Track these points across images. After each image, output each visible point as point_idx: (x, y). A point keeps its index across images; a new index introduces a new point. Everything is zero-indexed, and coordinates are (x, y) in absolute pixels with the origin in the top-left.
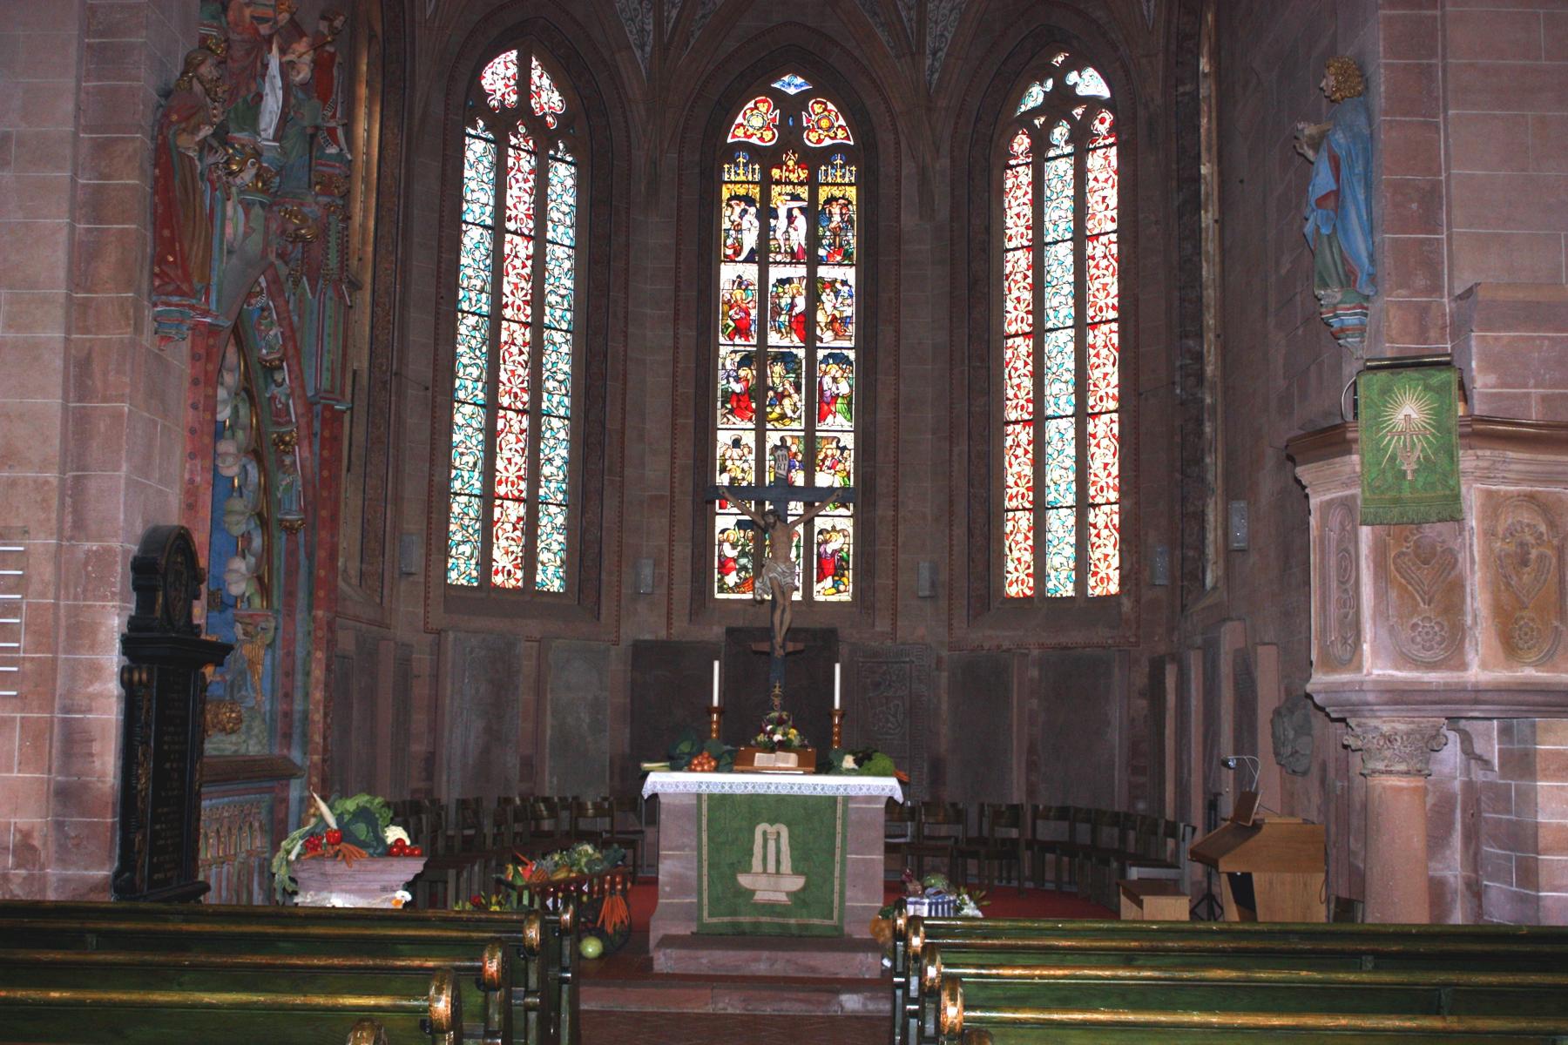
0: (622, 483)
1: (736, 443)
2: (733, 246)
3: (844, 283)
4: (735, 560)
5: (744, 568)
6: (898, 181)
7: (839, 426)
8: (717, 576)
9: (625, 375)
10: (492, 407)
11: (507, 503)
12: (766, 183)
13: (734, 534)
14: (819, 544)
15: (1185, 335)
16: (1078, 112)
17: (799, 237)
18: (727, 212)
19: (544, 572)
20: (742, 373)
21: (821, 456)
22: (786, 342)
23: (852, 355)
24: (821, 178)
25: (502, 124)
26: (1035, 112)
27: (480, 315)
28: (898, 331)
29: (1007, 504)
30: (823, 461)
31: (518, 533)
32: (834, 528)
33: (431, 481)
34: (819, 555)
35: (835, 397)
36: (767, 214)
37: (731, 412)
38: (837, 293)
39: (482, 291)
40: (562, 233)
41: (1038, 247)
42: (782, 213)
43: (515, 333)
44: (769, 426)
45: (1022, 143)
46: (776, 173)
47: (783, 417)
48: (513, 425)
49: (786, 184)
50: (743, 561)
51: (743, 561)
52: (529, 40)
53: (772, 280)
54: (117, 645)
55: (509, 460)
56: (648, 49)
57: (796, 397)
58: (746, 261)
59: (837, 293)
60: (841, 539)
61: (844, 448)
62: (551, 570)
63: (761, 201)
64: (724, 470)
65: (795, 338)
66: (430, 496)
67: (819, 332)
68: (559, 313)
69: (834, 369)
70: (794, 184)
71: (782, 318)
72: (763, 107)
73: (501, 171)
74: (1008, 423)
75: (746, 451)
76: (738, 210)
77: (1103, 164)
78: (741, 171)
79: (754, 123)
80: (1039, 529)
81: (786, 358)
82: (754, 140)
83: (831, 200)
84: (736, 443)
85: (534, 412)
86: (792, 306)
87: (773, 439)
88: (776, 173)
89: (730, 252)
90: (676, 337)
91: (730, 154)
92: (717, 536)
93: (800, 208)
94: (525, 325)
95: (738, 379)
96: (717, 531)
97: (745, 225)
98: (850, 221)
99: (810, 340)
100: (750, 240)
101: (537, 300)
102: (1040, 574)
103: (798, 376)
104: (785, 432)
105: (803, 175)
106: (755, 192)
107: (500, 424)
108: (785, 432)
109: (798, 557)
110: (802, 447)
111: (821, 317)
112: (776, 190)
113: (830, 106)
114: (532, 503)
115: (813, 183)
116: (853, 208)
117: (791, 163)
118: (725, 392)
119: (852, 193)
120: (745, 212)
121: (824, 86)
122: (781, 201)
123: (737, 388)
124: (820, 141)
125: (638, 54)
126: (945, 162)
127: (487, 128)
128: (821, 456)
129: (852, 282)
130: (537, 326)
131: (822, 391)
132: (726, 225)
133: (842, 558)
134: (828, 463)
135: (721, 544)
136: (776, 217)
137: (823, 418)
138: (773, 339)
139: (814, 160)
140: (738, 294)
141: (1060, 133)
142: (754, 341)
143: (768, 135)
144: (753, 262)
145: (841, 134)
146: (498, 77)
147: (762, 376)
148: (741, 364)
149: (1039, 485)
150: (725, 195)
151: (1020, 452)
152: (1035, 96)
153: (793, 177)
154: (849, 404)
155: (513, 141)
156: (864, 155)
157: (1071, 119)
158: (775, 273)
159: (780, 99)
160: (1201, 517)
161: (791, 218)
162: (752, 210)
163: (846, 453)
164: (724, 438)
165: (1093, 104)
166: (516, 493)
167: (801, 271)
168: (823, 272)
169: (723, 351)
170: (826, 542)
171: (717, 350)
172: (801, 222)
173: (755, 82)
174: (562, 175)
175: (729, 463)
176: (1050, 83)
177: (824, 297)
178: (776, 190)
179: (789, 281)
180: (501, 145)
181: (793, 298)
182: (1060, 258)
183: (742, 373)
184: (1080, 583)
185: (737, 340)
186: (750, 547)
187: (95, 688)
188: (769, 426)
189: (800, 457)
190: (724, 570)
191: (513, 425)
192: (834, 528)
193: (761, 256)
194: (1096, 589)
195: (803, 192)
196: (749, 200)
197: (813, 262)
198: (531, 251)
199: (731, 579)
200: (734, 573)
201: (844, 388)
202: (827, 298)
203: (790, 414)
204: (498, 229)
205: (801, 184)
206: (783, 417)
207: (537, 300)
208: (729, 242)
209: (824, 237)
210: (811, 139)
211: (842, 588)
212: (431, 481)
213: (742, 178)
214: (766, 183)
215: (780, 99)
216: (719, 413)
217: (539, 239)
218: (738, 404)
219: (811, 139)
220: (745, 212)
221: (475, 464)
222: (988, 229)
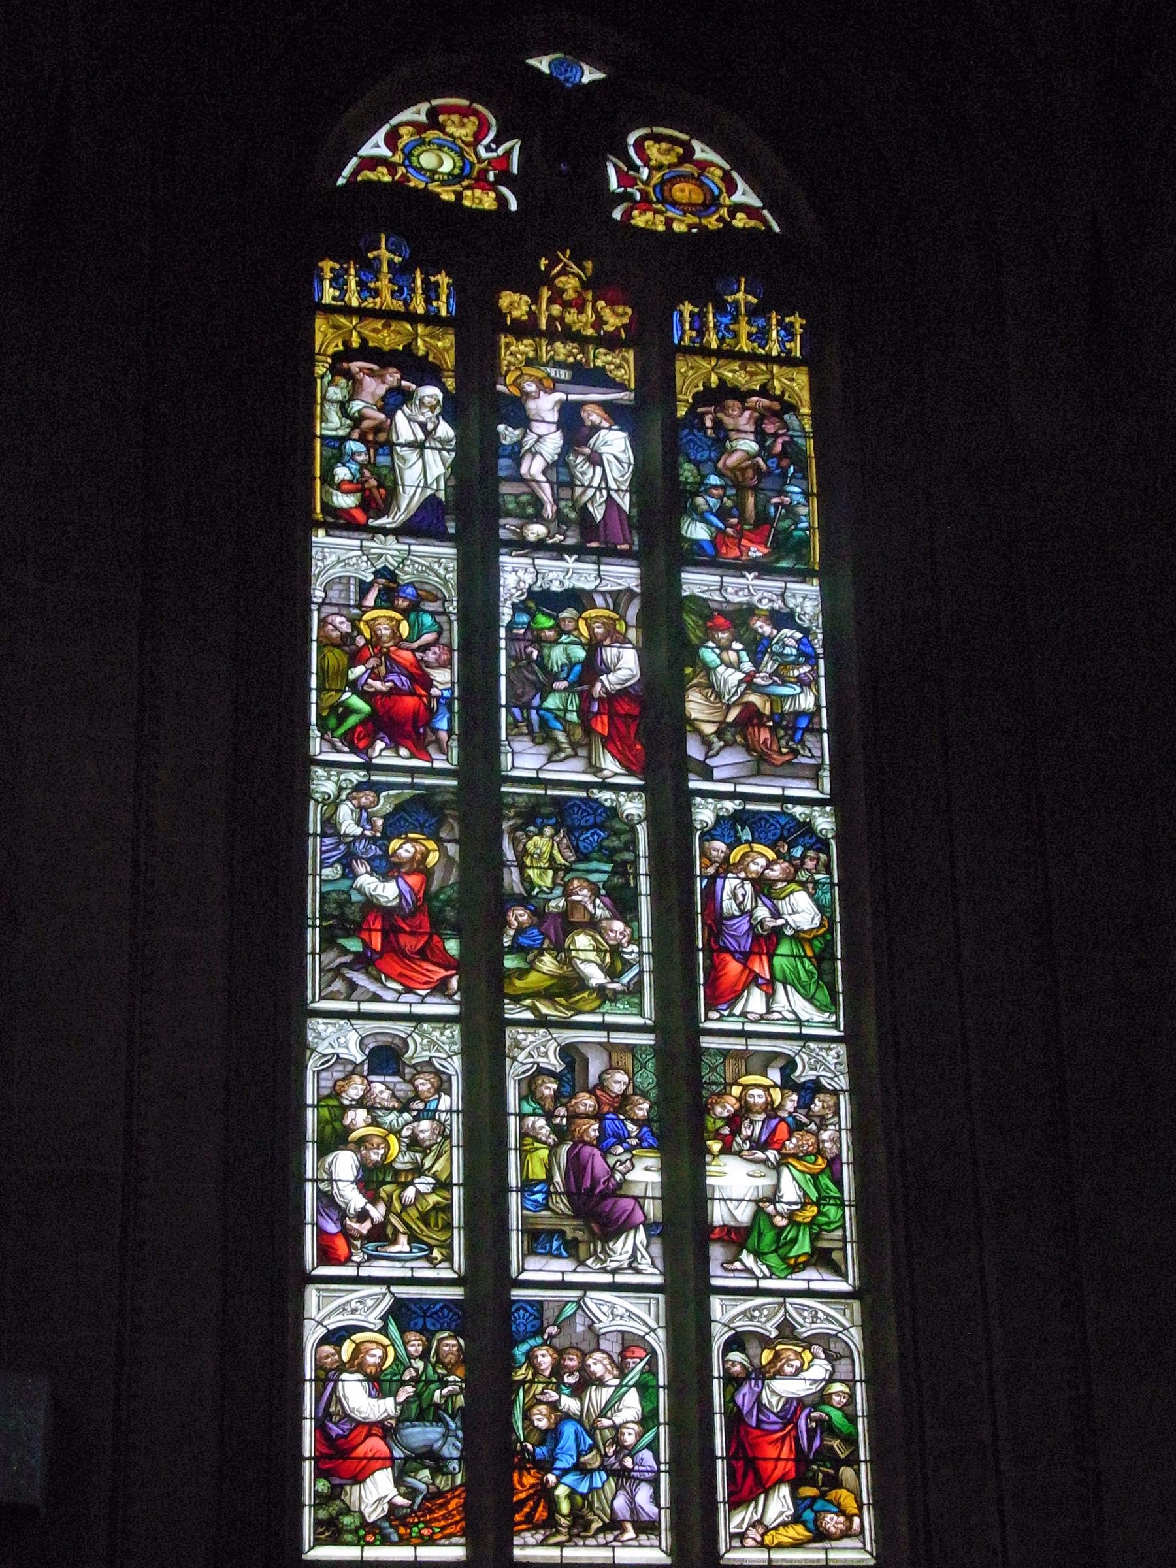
2: (356, 485)
4: (385, 1430)
5: (431, 1458)
7: (786, 1020)
8: (310, 1484)
14: (732, 1381)
20: (404, 850)
21: (726, 1108)
22: (571, 771)
23: (824, 823)
30: (735, 1121)
32: (787, 1331)
34: (735, 1418)
37: (363, 961)
38: (758, 648)
44: (513, 1012)
49: (552, 335)
50: (423, 1435)
51: (423, 1435)
60: (820, 1370)
61: (815, 1088)
63: (461, 371)
64: (335, 1138)
65: (610, 764)
67: (694, 749)
71: (552, 702)
72: (463, 131)
75: (424, 1085)
76: (374, 388)
78: (384, 284)
86: (593, 668)
87: (532, 1050)
93: (605, 406)
96: (312, 1334)
97: (404, 428)
98: (792, 452)
100: (423, 474)
103: (624, 870)
104: (593, 1011)
109: (647, 1420)
110: (647, 1079)
116: (803, 421)
117: (570, 284)
123: (387, 892)
128: (726, 1108)
131: (716, 921)
133: (827, 1427)
134: (754, 1128)
135: (327, 1377)
136: (523, 421)
137: (723, 996)
138: (523, 759)
144: (440, 536)
150: (325, 336)
154: (823, 958)
161: (572, 423)
167: (624, 575)
169: (324, 784)
170: (761, 1374)
171: (307, 777)
178: (514, 351)
179: (578, 599)
181: (594, 646)
183: (404, 850)
186: (451, 1389)
190: (342, 1458)
192: (787, 1331)
195: (622, 365)
199: (377, 1492)
201: (801, 911)
203: (596, 976)
205: (611, 342)
206: (569, 985)
209: (701, 488)
211: (833, 1522)
213: (387, 301)
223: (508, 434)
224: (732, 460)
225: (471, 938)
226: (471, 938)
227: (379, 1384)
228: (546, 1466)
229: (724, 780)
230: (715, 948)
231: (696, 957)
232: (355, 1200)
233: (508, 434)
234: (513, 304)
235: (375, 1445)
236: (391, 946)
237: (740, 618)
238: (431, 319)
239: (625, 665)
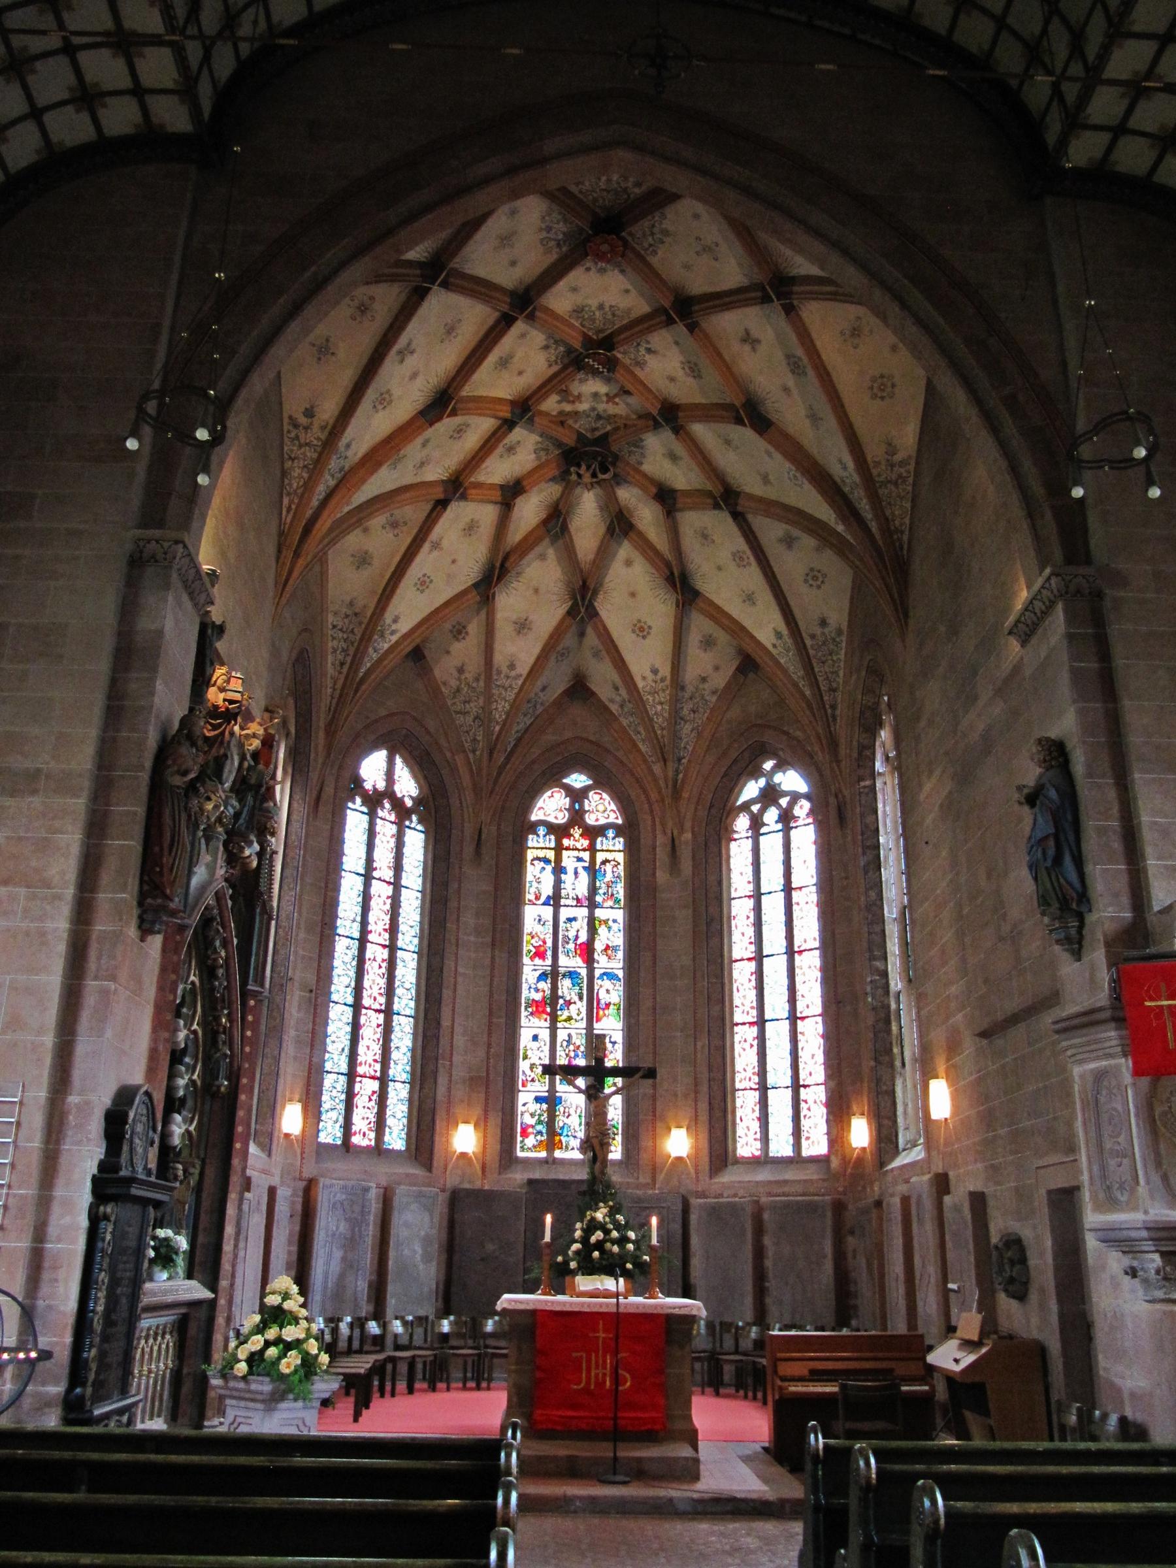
0: (451, 1065)
1: (535, 1038)
3: (615, 921)
5: (540, 1133)
6: (654, 848)
8: (519, 1139)
9: (455, 985)
10: (357, 1006)
11: (364, 1080)
12: (559, 849)
13: (534, 1107)
15: (872, 958)
16: (784, 802)
17: (582, 889)
18: (529, 868)
19: (391, 1133)
23: (620, 974)
24: (598, 847)
25: (373, 801)
26: (752, 801)
27: (352, 938)
28: (654, 956)
29: (738, 1085)
31: (373, 1103)
33: (311, 1061)
35: (608, 1005)
36: (559, 870)
37: (532, 1014)
38: (609, 928)
39: (354, 921)
40: (413, 877)
41: (757, 896)
42: (570, 871)
43: (376, 953)
45: (742, 823)
46: (566, 842)
47: (569, 1019)
48: (372, 1022)
50: (539, 1127)
51: (539, 1127)
52: (396, 744)
53: (562, 918)
54: (88, 1184)
55: (368, 1047)
56: (478, 753)
57: (579, 1003)
58: (544, 904)
59: (609, 928)
62: (395, 1135)
64: (525, 1057)
66: (310, 1073)
67: (596, 956)
68: (409, 938)
69: (607, 984)
70: (577, 849)
73: (372, 834)
74: (737, 1024)
77: (805, 837)
78: (541, 840)
79: (551, 806)
80: (764, 1103)
81: (572, 975)
82: (551, 819)
83: (604, 862)
84: (535, 1038)
85: (388, 1012)
86: (577, 937)
87: (562, 1035)
88: (566, 842)
89: (532, 897)
90: (493, 958)
91: (533, 828)
92: (520, 1109)
94: (384, 946)
95: (537, 990)
96: (520, 1102)
99: (589, 960)
100: (547, 890)
101: (393, 929)
102: (765, 1139)
105: (586, 843)
106: (551, 855)
107: (363, 1020)
108: (573, 1030)
110: (584, 1041)
111: (599, 946)
112: (565, 853)
113: (605, 796)
114: (384, 1080)
115: (592, 849)
116: (621, 867)
117: (577, 836)
118: (528, 999)
119: (620, 857)
120: (544, 868)
121: (602, 781)
122: (568, 860)
123: (538, 997)
124: (597, 820)
125: (471, 756)
126: (688, 836)
127: (363, 804)
129: (620, 919)
130: (392, 948)
131: (598, 1001)
132: (529, 877)
138: (563, 961)
139: (593, 833)
140: (538, 929)
141: (771, 816)
142: (549, 961)
143: (560, 815)
145: (613, 816)
146: (373, 768)
147: (554, 988)
148: (539, 979)
149: (762, 1072)
150: (530, 854)
151: (747, 1046)
152: (751, 790)
153: (579, 846)
154: (618, 1009)
155: (380, 813)
156: (628, 830)
157: (779, 806)
158: (564, 913)
159: (569, 791)
160: (893, 1093)
161: (576, 873)
162: (549, 868)
163: (616, 1046)
164: (525, 1036)
165: (795, 797)
166: (373, 1073)
168: (599, 913)
172: (584, 877)
173: (552, 777)
174: (415, 841)
175: (529, 1053)
176: (762, 782)
177: (600, 931)
178: (565, 853)
179: (575, 919)
180: (372, 815)
182: (773, 907)
184: (797, 1145)
185: (537, 961)
186: (545, 1117)
187: (67, 1220)
188: (559, 1025)
189: (582, 1049)
190: (525, 1134)
191: (372, 1022)
193: (555, 900)
194: (808, 1150)
195: (586, 855)
196: (546, 861)
197: (592, 905)
198: (390, 893)
199: (530, 1141)
200: (532, 1137)
202: (602, 930)
203: (575, 1016)
204: (368, 876)
205: (584, 850)
207: (393, 929)
208: (533, 890)
209: (600, 888)
210: (590, 820)
212: (311, 1061)
214: (559, 849)
215: (569, 791)
216: (524, 1013)
217: (397, 885)
218: (537, 1008)
219: (590, 820)
220: (544, 868)
221: (343, 1050)
222: (720, 883)
223: (563, 876)
224: (606, 880)
225: (550, 1007)
226: (550, 1007)
227: (532, 1115)
228: (560, 1135)
229: (602, 963)
230: (598, 1008)
231: (594, 1010)
232: (528, 1072)
233: (563, 876)
235: (530, 1130)
236: (537, 1011)
237: (606, 922)
239: (583, 938)
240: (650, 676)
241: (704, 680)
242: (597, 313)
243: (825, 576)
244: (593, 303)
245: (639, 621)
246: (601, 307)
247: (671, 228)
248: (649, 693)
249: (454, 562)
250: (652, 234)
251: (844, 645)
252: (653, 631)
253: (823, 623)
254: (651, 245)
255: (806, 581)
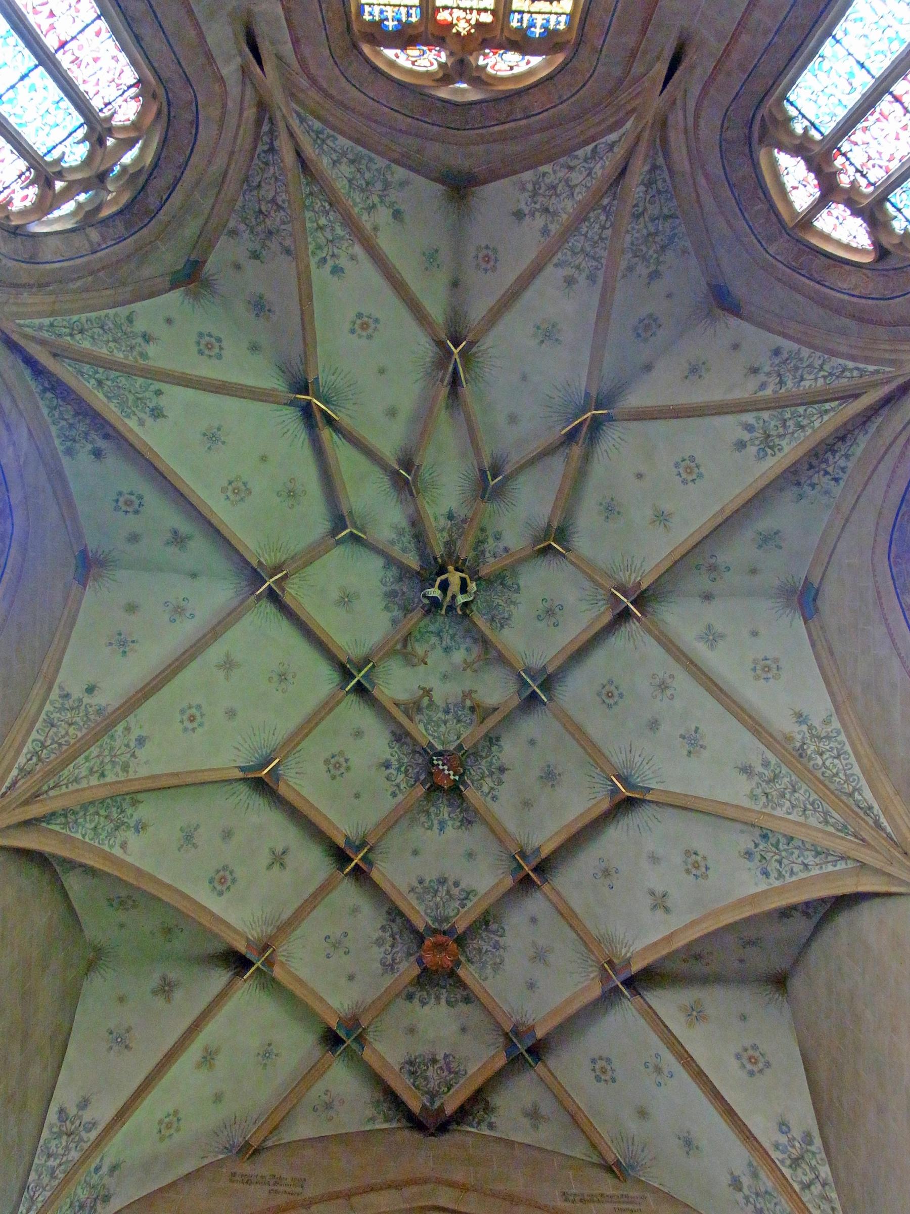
234: (487, 18)
238: (521, 12)
240: (343, 262)
241: (255, 255)
242: (446, 816)
243: (117, 509)
244: (451, 831)
245: (370, 337)
246: (442, 826)
247: (375, 949)
248: (342, 238)
249: (640, 476)
250: (393, 936)
251: (57, 442)
252: (347, 326)
253: (97, 454)
254: (393, 921)
255: (140, 497)
